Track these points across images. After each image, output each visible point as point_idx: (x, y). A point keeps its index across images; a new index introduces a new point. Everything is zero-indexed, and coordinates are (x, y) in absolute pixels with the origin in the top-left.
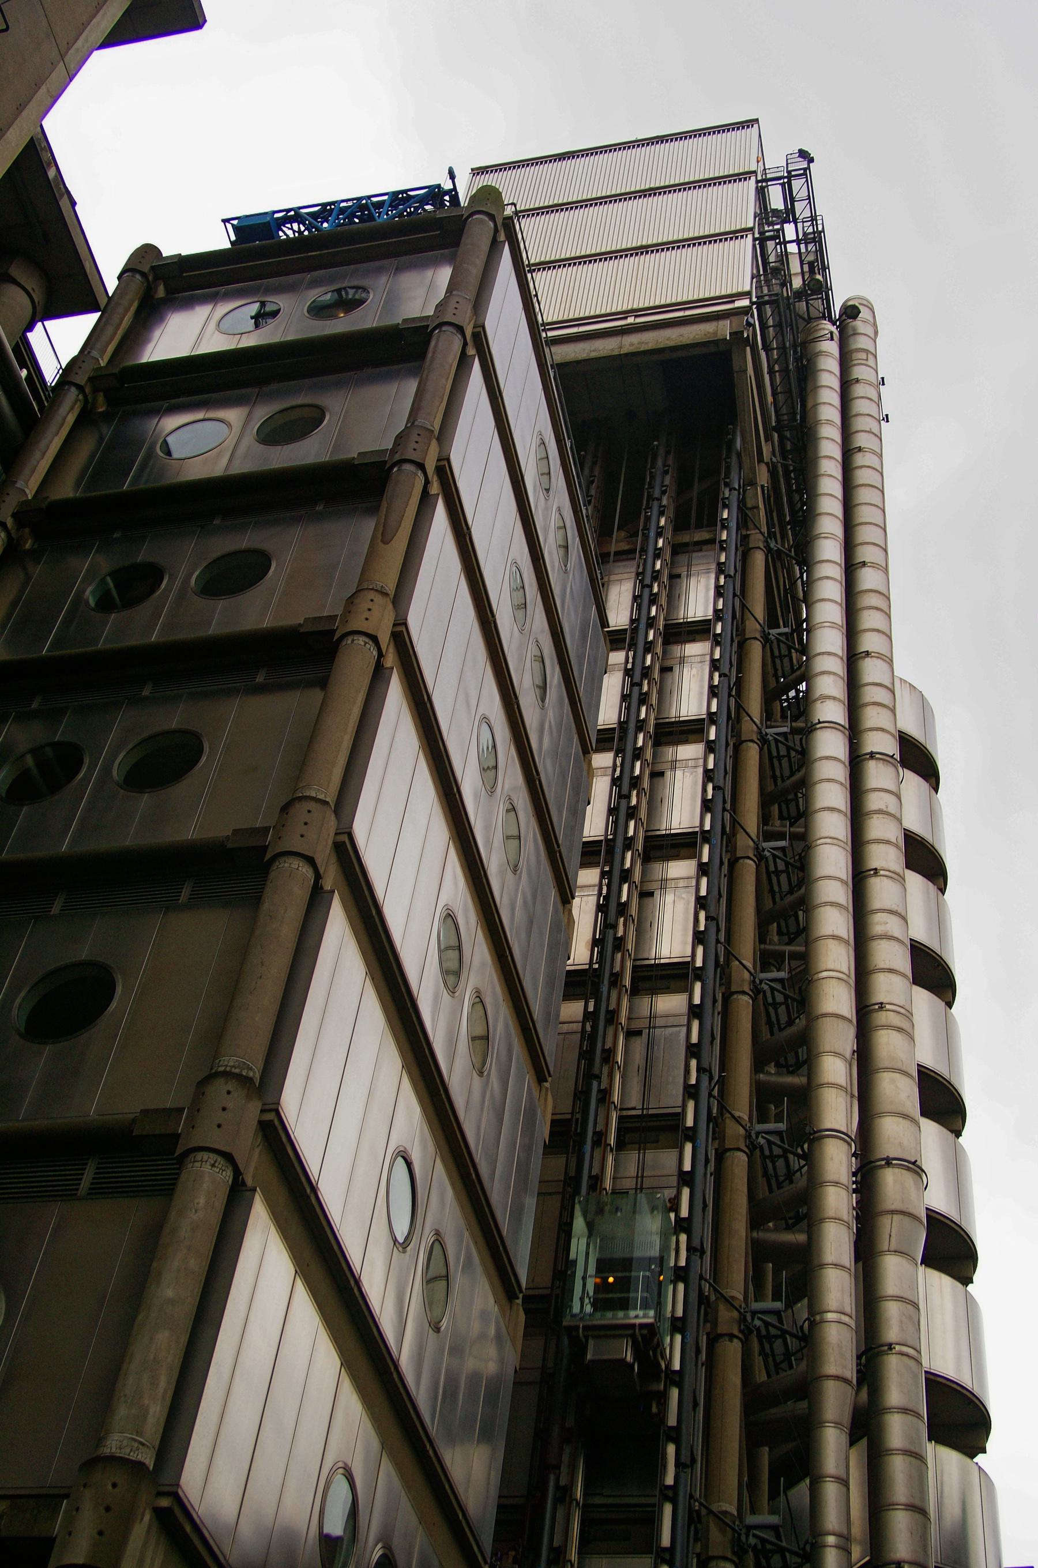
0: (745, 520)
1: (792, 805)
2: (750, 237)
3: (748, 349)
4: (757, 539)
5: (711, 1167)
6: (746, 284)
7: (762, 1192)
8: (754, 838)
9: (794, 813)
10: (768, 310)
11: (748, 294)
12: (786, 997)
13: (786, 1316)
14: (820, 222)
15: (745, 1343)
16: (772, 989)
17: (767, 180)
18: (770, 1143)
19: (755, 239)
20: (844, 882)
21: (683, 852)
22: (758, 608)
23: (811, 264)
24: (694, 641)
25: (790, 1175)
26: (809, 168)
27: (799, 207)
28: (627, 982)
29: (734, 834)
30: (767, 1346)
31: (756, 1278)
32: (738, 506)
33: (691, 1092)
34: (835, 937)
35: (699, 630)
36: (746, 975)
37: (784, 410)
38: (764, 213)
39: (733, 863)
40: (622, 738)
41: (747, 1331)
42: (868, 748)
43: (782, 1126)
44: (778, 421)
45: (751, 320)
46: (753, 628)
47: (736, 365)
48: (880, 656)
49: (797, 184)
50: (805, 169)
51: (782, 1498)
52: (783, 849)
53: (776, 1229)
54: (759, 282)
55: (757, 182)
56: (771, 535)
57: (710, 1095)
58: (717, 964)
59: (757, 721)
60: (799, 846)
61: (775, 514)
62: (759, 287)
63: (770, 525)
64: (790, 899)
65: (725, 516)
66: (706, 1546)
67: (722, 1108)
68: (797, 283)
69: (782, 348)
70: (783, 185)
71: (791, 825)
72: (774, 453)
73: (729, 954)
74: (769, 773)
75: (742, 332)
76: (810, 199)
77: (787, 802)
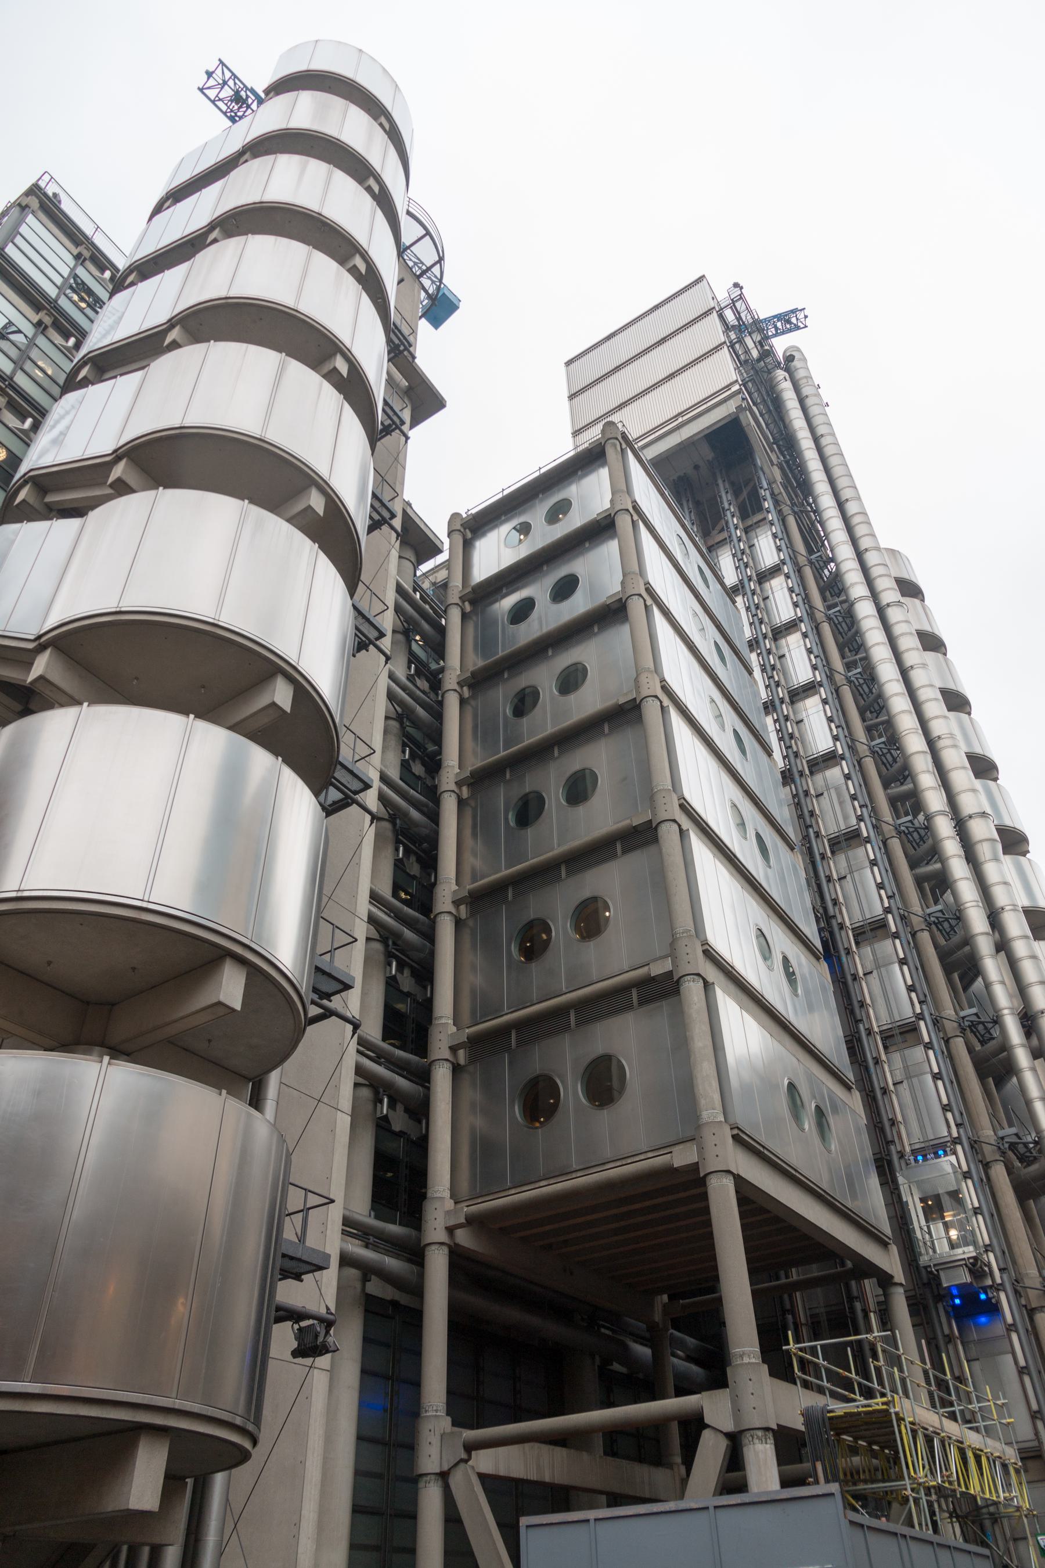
0: (777, 503)
2: (725, 347)
3: (747, 412)
4: (786, 510)
5: (883, 850)
6: (732, 375)
7: (912, 851)
8: (843, 673)
9: (837, 591)
11: (737, 381)
12: (864, 680)
13: (916, 822)
14: (755, 314)
15: (930, 932)
16: (857, 678)
17: (722, 309)
18: (907, 828)
19: (728, 347)
20: (898, 681)
21: (792, 630)
22: (800, 547)
23: (760, 342)
24: (773, 578)
25: (895, 760)
27: (743, 315)
28: (807, 772)
29: (832, 674)
30: (940, 927)
32: (772, 498)
33: (860, 819)
34: (903, 712)
35: (775, 571)
36: (866, 747)
37: (775, 432)
38: (727, 328)
39: (837, 690)
40: (743, 587)
41: (899, 833)
43: (883, 739)
44: (773, 438)
45: (744, 396)
46: (802, 560)
47: (744, 423)
48: (853, 499)
49: (738, 305)
50: (740, 295)
52: (839, 611)
54: (740, 371)
55: (717, 312)
56: (793, 504)
57: (870, 817)
59: (822, 610)
60: (845, 606)
61: (789, 488)
62: (741, 374)
63: (791, 499)
64: (850, 634)
65: (767, 506)
66: (945, 1033)
67: (878, 820)
68: (755, 354)
69: (764, 400)
70: (731, 307)
72: (778, 458)
73: (853, 740)
74: (837, 632)
75: (741, 405)
76: (748, 308)
77: (832, 588)
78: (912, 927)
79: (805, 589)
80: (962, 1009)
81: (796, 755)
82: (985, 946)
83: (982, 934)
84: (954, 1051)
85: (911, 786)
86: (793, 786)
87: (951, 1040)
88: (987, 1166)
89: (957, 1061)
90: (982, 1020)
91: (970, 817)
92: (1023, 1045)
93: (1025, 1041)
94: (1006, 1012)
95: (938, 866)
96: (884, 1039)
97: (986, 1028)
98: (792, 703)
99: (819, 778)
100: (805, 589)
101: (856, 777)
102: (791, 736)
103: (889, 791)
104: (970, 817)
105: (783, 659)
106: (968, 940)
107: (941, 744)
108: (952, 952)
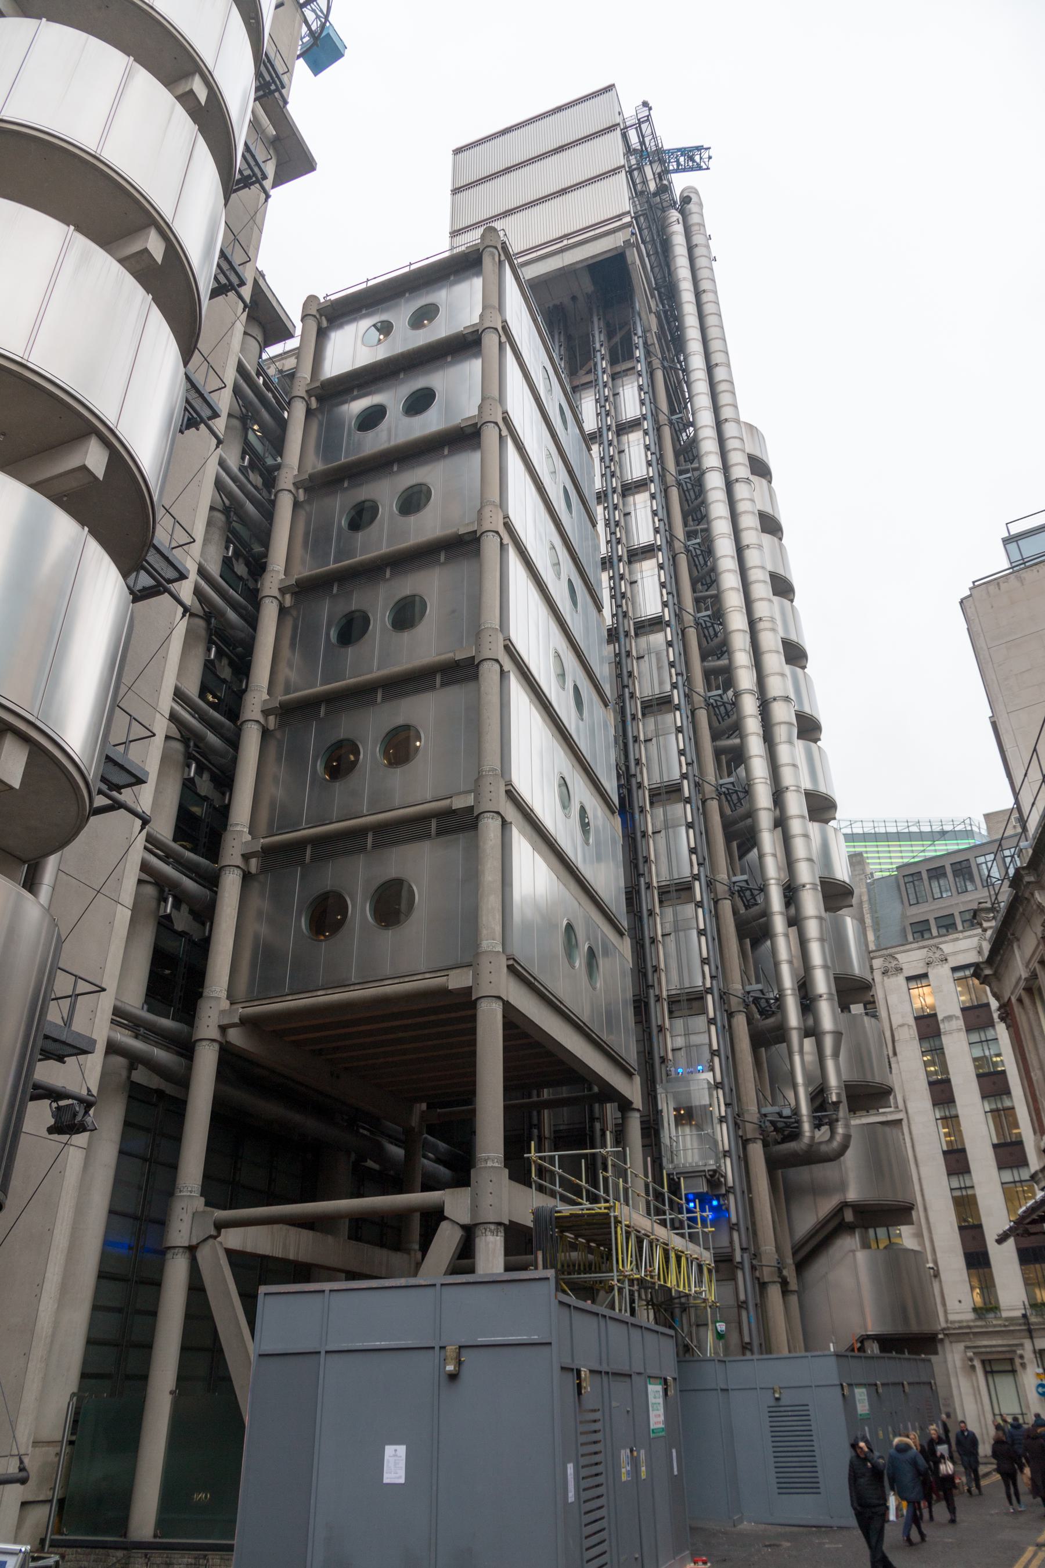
0: (648, 353)
1: (690, 453)
2: (624, 171)
4: (656, 363)
5: (690, 719)
6: (626, 206)
7: (716, 724)
8: (683, 541)
9: (691, 458)
10: (642, 219)
11: (629, 212)
12: (702, 551)
13: (725, 697)
14: (659, 141)
16: (695, 548)
17: (626, 128)
18: (716, 701)
19: (626, 172)
20: (733, 557)
21: (642, 489)
23: (659, 174)
25: (716, 635)
26: (650, 115)
27: (647, 140)
28: (633, 633)
29: (672, 540)
30: (729, 798)
31: (709, 687)
33: (674, 686)
34: (732, 589)
35: (634, 425)
36: (691, 617)
37: (659, 277)
38: (629, 151)
39: (674, 557)
40: (601, 436)
41: (708, 705)
42: (734, 477)
43: (709, 613)
44: (656, 284)
45: (634, 231)
46: (663, 419)
48: (722, 364)
49: (644, 126)
50: (648, 116)
51: (734, 773)
52: (690, 478)
53: (713, 661)
54: (634, 202)
55: (621, 130)
56: (664, 358)
57: (684, 685)
58: (667, 542)
59: (674, 474)
60: (696, 473)
62: (635, 206)
63: (662, 352)
65: (638, 355)
66: (716, 894)
67: (690, 689)
68: (652, 186)
70: (636, 128)
71: (691, 463)
72: (657, 305)
73: (680, 609)
77: (687, 453)
78: (704, 795)
79: (661, 449)
80: (735, 875)
81: (625, 615)
82: (765, 820)
83: (765, 809)
84: (720, 912)
85: (726, 662)
86: (617, 645)
87: (720, 902)
88: (730, 1015)
89: (722, 921)
90: (751, 887)
91: (775, 699)
92: (781, 913)
93: (784, 910)
94: (772, 882)
95: (737, 741)
96: (660, 894)
97: (752, 894)
98: (630, 562)
99: (643, 641)
100: (661, 449)
101: (678, 645)
102: (623, 595)
103: (706, 664)
104: (775, 699)
105: (628, 517)
106: (751, 814)
107: (761, 625)
108: (735, 822)
